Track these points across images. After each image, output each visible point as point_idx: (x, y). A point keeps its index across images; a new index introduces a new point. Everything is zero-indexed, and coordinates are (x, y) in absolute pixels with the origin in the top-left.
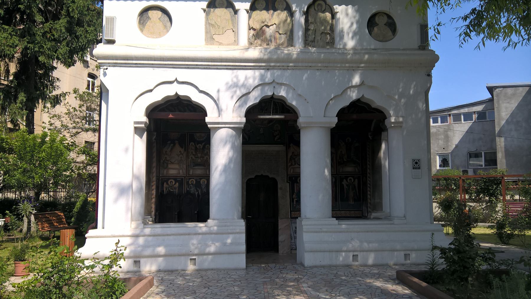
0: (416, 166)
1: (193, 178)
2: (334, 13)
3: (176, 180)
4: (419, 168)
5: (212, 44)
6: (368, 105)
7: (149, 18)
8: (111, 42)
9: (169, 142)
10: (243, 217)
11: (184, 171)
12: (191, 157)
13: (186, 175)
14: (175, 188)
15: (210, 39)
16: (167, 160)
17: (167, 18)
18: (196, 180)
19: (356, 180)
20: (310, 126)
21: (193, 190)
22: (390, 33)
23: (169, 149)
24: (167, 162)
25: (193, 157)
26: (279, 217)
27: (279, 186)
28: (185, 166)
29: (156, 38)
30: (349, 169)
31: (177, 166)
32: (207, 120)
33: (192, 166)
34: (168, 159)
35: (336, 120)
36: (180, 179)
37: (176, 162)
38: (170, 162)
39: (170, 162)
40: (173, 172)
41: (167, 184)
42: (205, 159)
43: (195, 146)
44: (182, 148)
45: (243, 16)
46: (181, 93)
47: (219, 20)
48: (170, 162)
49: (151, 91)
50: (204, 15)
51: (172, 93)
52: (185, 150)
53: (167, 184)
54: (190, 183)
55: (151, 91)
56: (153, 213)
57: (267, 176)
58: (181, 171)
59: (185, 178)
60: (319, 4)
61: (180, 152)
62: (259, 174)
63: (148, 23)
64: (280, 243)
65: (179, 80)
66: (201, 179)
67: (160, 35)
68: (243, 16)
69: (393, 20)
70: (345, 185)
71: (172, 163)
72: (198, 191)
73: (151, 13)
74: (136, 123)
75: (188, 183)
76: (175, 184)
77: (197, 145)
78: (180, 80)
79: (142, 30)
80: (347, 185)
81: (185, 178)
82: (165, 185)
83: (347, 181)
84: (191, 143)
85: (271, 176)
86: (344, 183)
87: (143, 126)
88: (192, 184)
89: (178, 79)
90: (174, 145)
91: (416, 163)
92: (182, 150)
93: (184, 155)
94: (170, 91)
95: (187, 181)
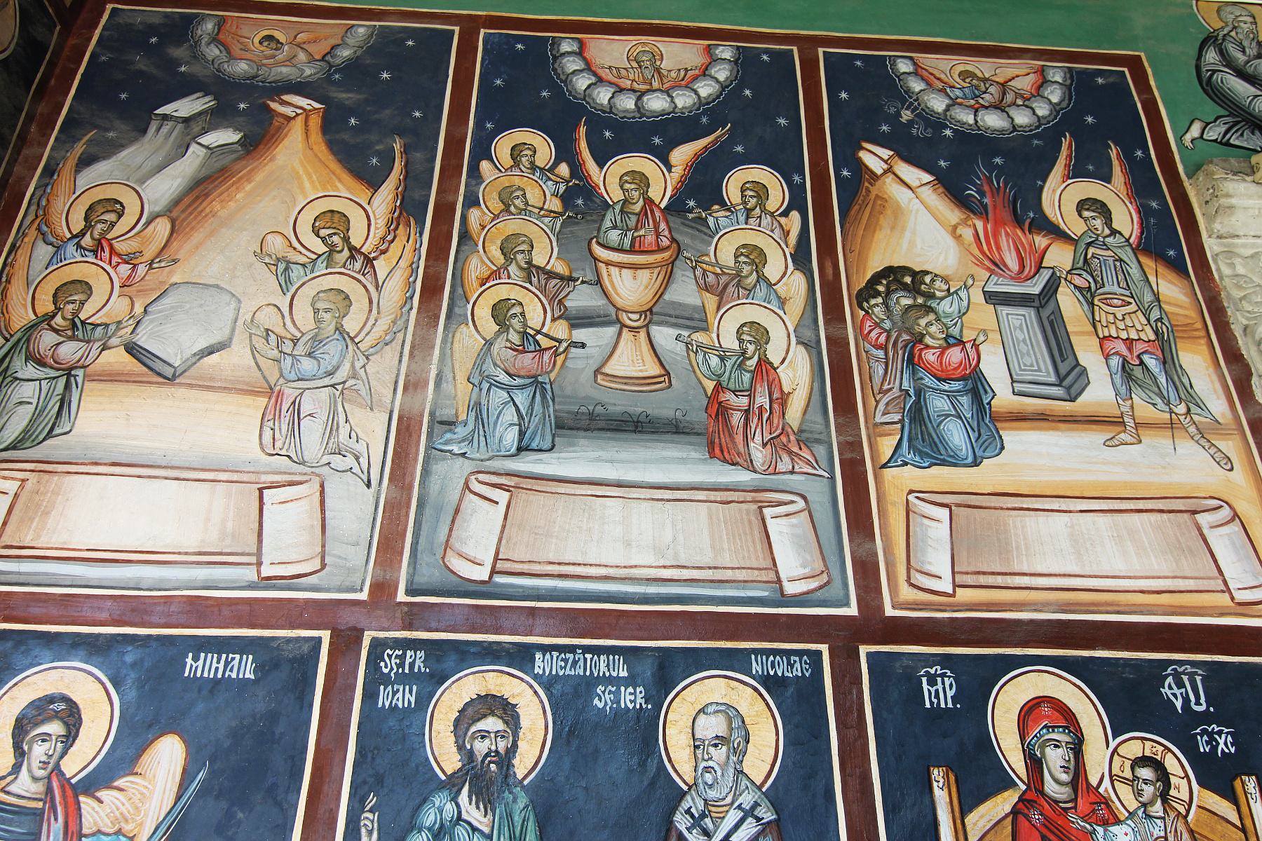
1: (521, 657)
9: (185, 107)
12: (500, 312)
13: (382, 589)
16: (77, 328)
24: (69, 351)
25: (535, 314)
33: (511, 438)
36: (244, 668)
37: (237, 360)
38: (132, 349)
39: (116, 358)
42: (730, 342)
43: (564, 169)
44: (373, 182)
48: (132, 349)
54: (445, 756)
59: (346, 642)
61: (334, 221)
77: (601, 165)
81: (346, 642)
84: (503, 146)
93: (381, 266)
95: (384, 699)
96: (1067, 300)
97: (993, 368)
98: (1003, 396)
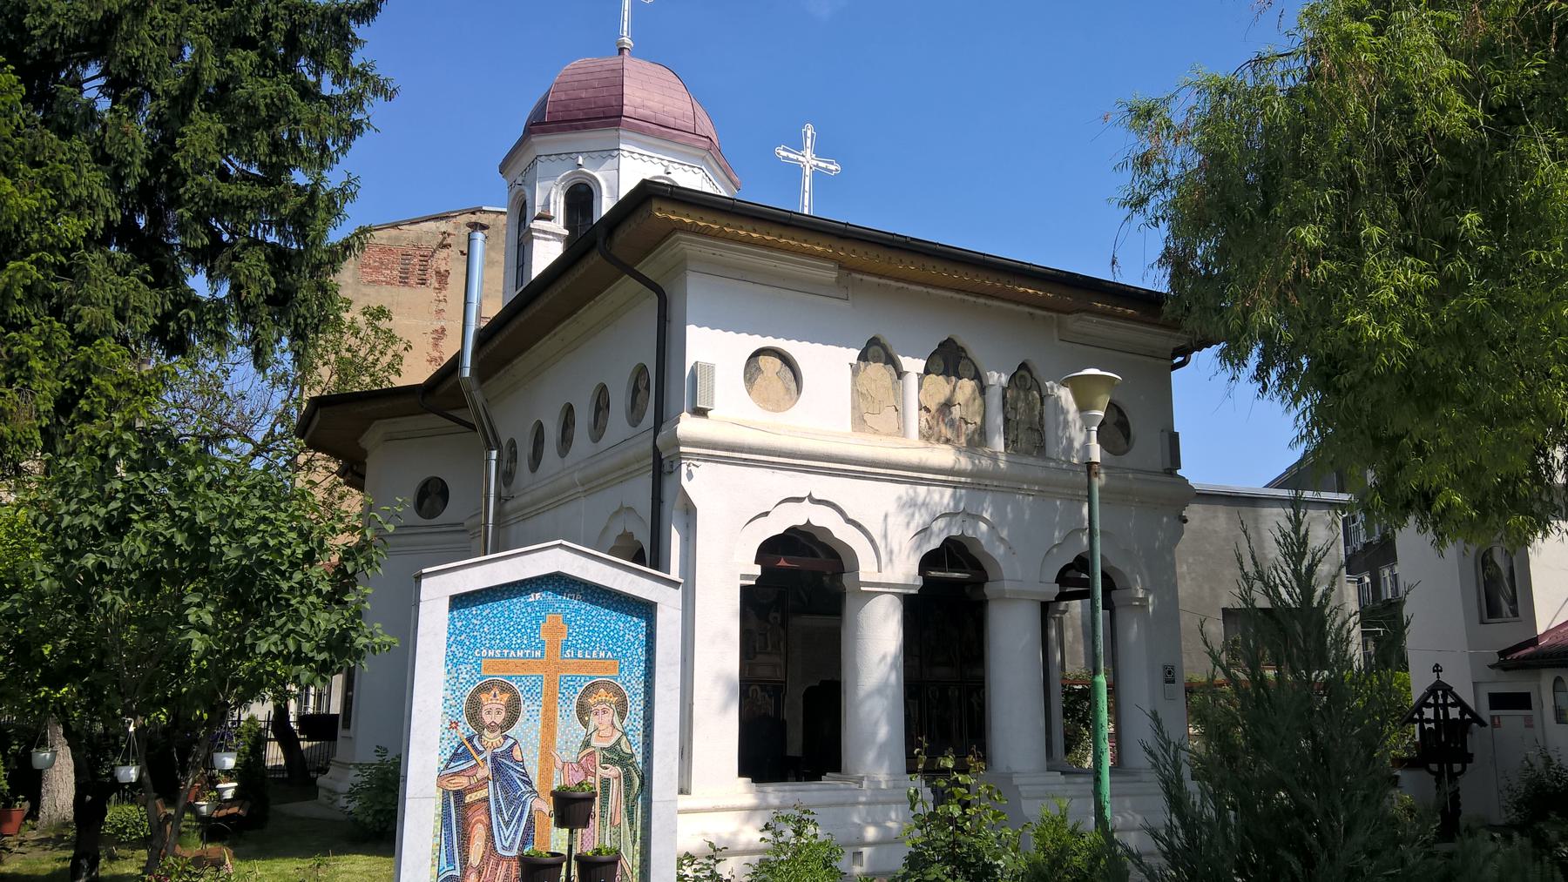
0: (1170, 677)
2: (1044, 394)
4: (1173, 682)
5: (862, 431)
7: (759, 369)
8: (701, 412)
17: (790, 375)
22: (1122, 441)
29: (773, 411)
45: (912, 381)
46: (815, 523)
47: (873, 386)
49: (767, 514)
50: (849, 372)
51: (801, 522)
55: (767, 514)
60: (1022, 376)
63: (759, 380)
67: (778, 407)
68: (912, 381)
69: (1125, 417)
70: (975, 704)
73: (762, 359)
74: (744, 577)
78: (816, 496)
89: (813, 495)
91: (1170, 673)
94: (797, 516)
96: (768, 635)
97: (757, 646)
98: (757, 650)
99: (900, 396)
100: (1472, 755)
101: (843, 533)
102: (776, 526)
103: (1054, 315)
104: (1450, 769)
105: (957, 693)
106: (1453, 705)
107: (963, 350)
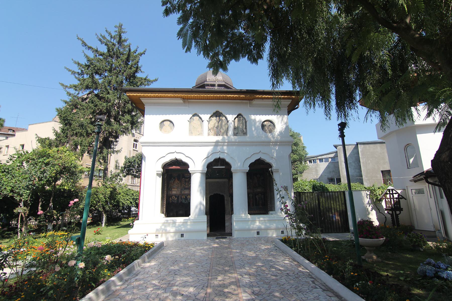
3: (175, 196)
6: (264, 161)
7: (164, 125)
10: (206, 214)
11: (180, 192)
14: (175, 200)
15: (191, 133)
18: (185, 196)
19: (263, 195)
20: (237, 171)
21: (183, 201)
23: (173, 182)
26: (226, 214)
27: (225, 199)
28: (180, 190)
30: (259, 190)
31: (176, 190)
32: (189, 169)
34: (172, 186)
35: (248, 169)
40: (174, 192)
41: (172, 198)
45: (205, 123)
49: (164, 157)
50: (188, 123)
52: (180, 182)
53: (172, 198)
56: (165, 213)
57: (220, 194)
58: (178, 192)
60: (240, 117)
62: (216, 193)
64: (226, 227)
65: (177, 152)
66: (187, 196)
68: (205, 123)
70: (257, 198)
71: (174, 188)
72: (186, 201)
73: (165, 122)
74: (157, 171)
75: (181, 198)
76: (175, 198)
79: (161, 130)
80: (258, 198)
82: (170, 199)
83: (258, 196)
85: (221, 194)
86: (257, 197)
87: (161, 172)
88: (183, 198)
90: (175, 180)
92: (179, 182)
99: (202, 126)
100: (402, 208)
101: (185, 160)
102: (167, 159)
103: (248, 101)
104: (395, 213)
105: (252, 195)
106: (395, 193)
107: (221, 113)
